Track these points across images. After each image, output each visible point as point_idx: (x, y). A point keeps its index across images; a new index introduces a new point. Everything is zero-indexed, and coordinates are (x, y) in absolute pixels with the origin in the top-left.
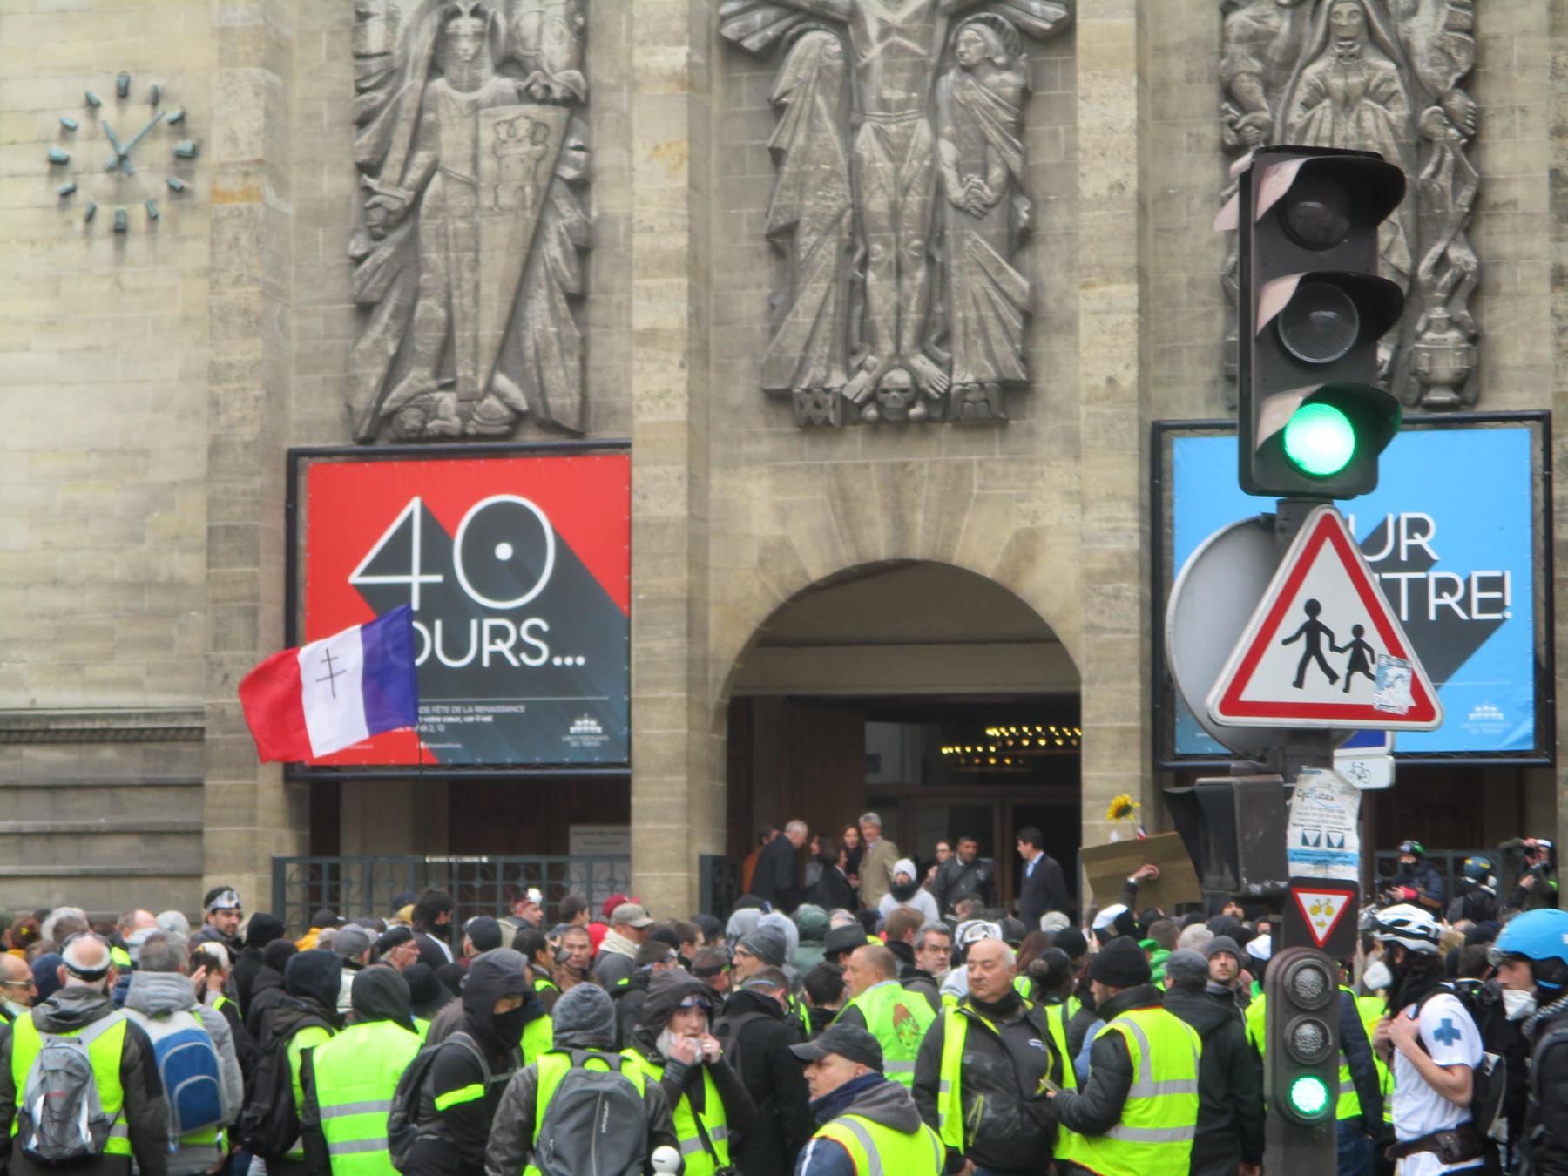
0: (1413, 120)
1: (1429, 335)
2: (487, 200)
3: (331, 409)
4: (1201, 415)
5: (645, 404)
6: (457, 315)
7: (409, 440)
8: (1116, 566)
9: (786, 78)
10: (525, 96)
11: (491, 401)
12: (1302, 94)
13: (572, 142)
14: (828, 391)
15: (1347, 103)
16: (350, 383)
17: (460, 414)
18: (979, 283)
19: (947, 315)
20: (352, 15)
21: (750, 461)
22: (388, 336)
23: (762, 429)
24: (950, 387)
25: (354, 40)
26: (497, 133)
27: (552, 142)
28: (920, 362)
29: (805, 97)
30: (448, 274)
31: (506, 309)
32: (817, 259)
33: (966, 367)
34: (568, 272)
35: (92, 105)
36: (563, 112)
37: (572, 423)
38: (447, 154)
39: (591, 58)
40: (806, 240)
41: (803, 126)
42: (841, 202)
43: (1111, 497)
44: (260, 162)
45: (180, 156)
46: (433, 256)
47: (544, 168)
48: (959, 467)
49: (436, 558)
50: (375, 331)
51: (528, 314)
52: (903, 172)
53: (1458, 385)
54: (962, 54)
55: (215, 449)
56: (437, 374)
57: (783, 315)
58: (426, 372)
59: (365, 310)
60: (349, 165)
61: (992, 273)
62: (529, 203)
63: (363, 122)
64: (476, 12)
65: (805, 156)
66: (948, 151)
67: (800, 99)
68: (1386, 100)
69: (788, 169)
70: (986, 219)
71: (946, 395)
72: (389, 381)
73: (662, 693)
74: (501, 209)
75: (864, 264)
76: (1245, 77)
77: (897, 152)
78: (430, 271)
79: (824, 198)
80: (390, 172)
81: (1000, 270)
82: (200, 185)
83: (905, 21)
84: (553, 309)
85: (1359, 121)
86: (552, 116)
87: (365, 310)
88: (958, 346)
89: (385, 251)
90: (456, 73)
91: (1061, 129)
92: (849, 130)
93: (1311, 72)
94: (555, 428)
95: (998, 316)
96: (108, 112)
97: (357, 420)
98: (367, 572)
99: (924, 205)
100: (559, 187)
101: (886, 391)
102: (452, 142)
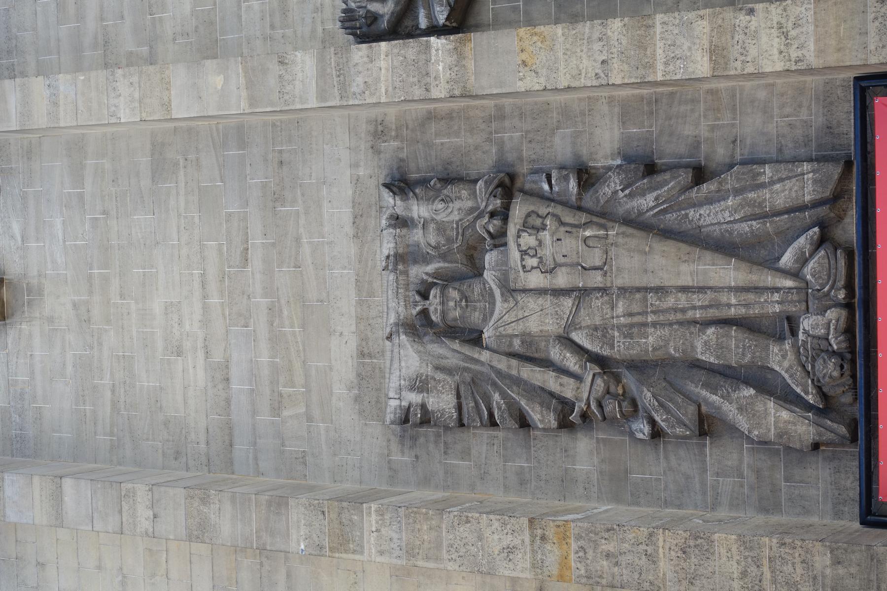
2: (596, 279)
5: (794, 55)
7: (854, 376)
10: (499, 239)
11: (808, 271)
13: (546, 187)
17: (822, 311)
22: (735, 395)
26: (533, 268)
27: (543, 211)
30: (671, 325)
31: (708, 255)
37: (835, 171)
38: (552, 326)
39: (473, 174)
44: (531, 521)
46: (653, 338)
47: (568, 218)
50: (730, 410)
51: (716, 231)
56: (781, 339)
58: (775, 349)
60: (564, 437)
62: (602, 232)
63: (524, 423)
64: (425, 296)
72: (788, 398)
74: (605, 264)
78: (667, 342)
80: (567, 389)
86: (519, 210)
89: (647, 397)
90: (477, 314)
97: (829, 436)
100: (588, 201)
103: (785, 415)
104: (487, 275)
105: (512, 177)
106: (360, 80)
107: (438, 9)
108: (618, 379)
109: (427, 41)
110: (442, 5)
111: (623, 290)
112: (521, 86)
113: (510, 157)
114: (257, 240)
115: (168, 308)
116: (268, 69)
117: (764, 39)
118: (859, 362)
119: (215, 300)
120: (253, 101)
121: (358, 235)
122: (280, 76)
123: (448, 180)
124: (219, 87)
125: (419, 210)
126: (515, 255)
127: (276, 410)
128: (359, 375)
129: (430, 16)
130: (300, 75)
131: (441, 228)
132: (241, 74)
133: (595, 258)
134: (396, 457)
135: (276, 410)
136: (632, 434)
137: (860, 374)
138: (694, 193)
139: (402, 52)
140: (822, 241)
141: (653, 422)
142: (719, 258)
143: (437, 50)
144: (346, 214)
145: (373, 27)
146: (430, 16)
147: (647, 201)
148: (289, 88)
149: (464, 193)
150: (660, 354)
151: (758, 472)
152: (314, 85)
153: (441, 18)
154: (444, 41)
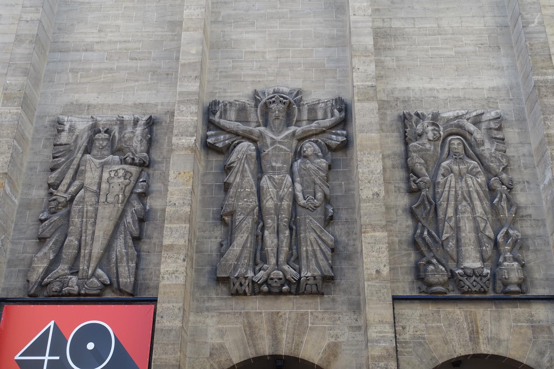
1: (506, 263)
2: (102, 199)
5: (165, 276)
6: (83, 243)
7: (53, 296)
8: (385, 353)
9: (233, 158)
10: (123, 161)
11: (94, 280)
13: (141, 180)
14: (246, 278)
16: (30, 267)
17: (77, 285)
19: (298, 249)
21: (208, 310)
22: (51, 251)
23: (214, 296)
24: (300, 278)
25: (55, 139)
26: (110, 175)
27: (132, 179)
28: (286, 267)
29: (240, 164)
30: (81, 227)
31: (105, 242)
32: (243, 225)
34: (134, 229)
38: (87, 181)
39: (152, 151)
40: (239, 217)
41: (239, 174)
42: (254, 203)
43: (381, 322)
44: (6, 174)
46: (76, 220)
47: (128, 189)
48: (302, 315)
49: (57, 349)
50: (46, 249)
51: (115, 245)
52: (280, 193)
53: (520, 285)
54: (304, 152)
56: (70, 269)
57: (228, 248)
58: (66, 267)
59: (42, 240)
61: (318, 232)
62: (120, 201)
63: (53, 170)
64: (106, 132)
65: (240, 186)
66: (298, 187)
67: (238, 165)
68: (476, 175)
69: (232, 191)
70: (315, 211)
71: (299, 281)
72: (47, 271)
74: (108, 203)
75: (263, 229)
76: (418, 164)
77: (278, 186)
78: (75, 226)
79: (247, 201)
80: (62, 188)
83: (281, 139)
84: (126, 243)
85: (466, 181)
86: (134, 170)
87: (42, 240)
88: (304, 262)
89: (55, 218)
90: (96, 152)
91: (343, 183)
93: (444, 164)
94: (121, 291)
95: (321, 249)
97: (31, 286)
98: (22, 355)
99: (289, 205)
100: (134, 196)
101: (272, 279)
103: (41, 270)
104: (111, 156)
105: (148, 166)
106: (184, 109)
107: (213, 139)
108: (64, 207)
109: (194, 135)
110: (214, 141)
111: (97, 210)
112: (171, 172)
113: (156, 166)
114: (139, 64)
115: (118, 26)
116: (195, 72)
117: (173, 265)
118: (56, 298)
119: (118, 46)
120: (183, 65)
121: (136, 105)
122: (191, 77)
124: (191, 52)
125: (139, 130)
126: (116, 168)
127: (72, 70)
128: (81, 104)
129: (212, 136)
130: (190, 84)
131: (131, 139)
132: (194, 61)
134: (47, 119)
135: (72, 70)
136: (43, 212)
137: (53, 298)
138: (129, 237)
139: (192, 126)
140: (105, 285)
141: (45, 220)
142: (104, 246)
143: (190, 140)
144: (144, 100)
145: (211, 113)
146: (212, 136)
148: (186, 80)
149: (143, 148)
150: (71, 223)
151: (23, 260)
152: (185, 90)
153: (209, 140)
154: (193, 142)
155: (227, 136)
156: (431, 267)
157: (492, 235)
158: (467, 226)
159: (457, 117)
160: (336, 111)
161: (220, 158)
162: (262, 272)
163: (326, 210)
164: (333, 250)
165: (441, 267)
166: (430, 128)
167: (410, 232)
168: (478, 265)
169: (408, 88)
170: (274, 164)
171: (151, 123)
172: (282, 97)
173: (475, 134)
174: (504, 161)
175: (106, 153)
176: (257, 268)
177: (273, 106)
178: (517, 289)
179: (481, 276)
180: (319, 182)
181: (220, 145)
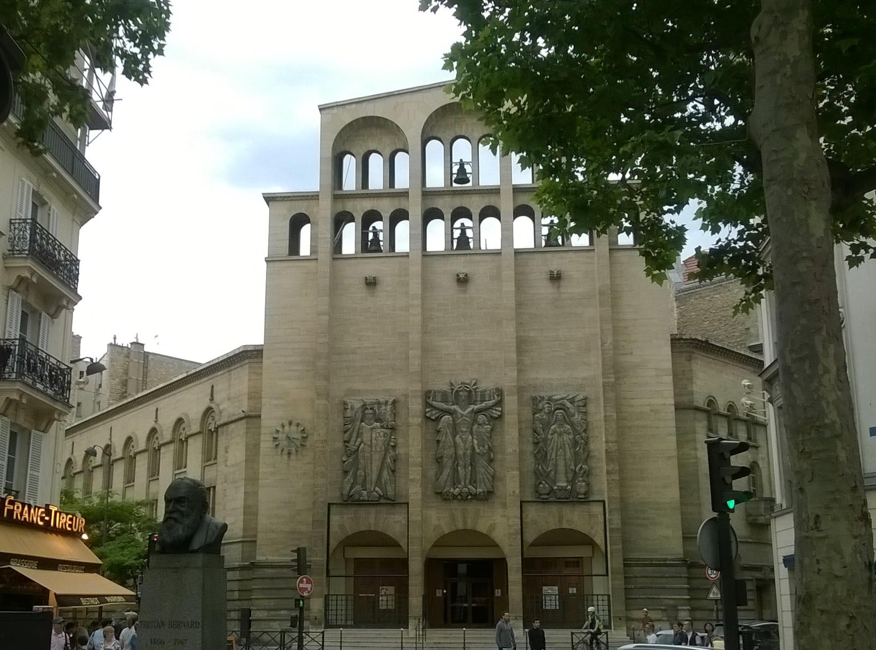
0: (574, 438)
2: (374, 450)
3: (338, 494)
4: (530, 500)
6: (367, 474)
7: (355, 501)
8: (515, 532)
10: (382, 427)
12: (550, 432)
13: (393, 437)
15: (560, 434)
16: (342, 488)
18: (483, 470)
20: (343, 408)
23: (434, 500)
25: (344, 414)
27: (388, 437)
33: (480, 488)
35: (283, 426)
36: (390, 431)
37: (393, 499)
38: (365, 439)
39: (396, 420)
40: (445, 460)
41: (444, 435)
45: (303, 437)
46: (362, 461)
47: (386, 443)
50: (348, 477)
55: (314, 503)
56: (362, 487)
57: (439, 477)
58: (360, 486)
59: (346, 472)
60: (342, 441)
63: (345, 432)
64: (371, 409)
65: (445, 442)
66: (475, 442)
68: (569, 434)
69: (441, 445)
72: (351, 489)
73: (416, 558)
77: (465, 442)
80: (352, 443)
81: (488, 467)
82: (308, 444)
84: (388, 473)
85: (563, 438)
86: (388, 431)
87: (346, 472)
88: (478, 484)
92: (454, 436)
93: (552, 427)
94: (389, 499)
96: (287, 428)
102: (366, 437)
103: (348, 488)
104: (375, 423)
111: (371, 455)
123: (395, 414)
129: (429, 411)
131: (385, 413)
133: (378, 449)
134: (337, 399)
147: (389, 461)
153: (428, 415)
155: (437, 411)
156: (542, 486)
157: (574, 468)
158: (561, 463)
159: (560, 399)
160: (496, 396)
161: (434, 423)
162: (457, 489)
163: (489, 455)
164: (493, 477)
165: (547, 485)
166: (547, 405)
167: (533, 465)
168: (565, 484)
169: (537, 378)
170: (462, 429)
171: (394, 402)
172: (466, 387)
173: (570, 409)
174: (584, 426)
175: (372, 422)
176: (455, 487)
177: (461, 393)
178: (583, 496)
179: (566, 490)
180: (486, 439)
181: (433, 418)
